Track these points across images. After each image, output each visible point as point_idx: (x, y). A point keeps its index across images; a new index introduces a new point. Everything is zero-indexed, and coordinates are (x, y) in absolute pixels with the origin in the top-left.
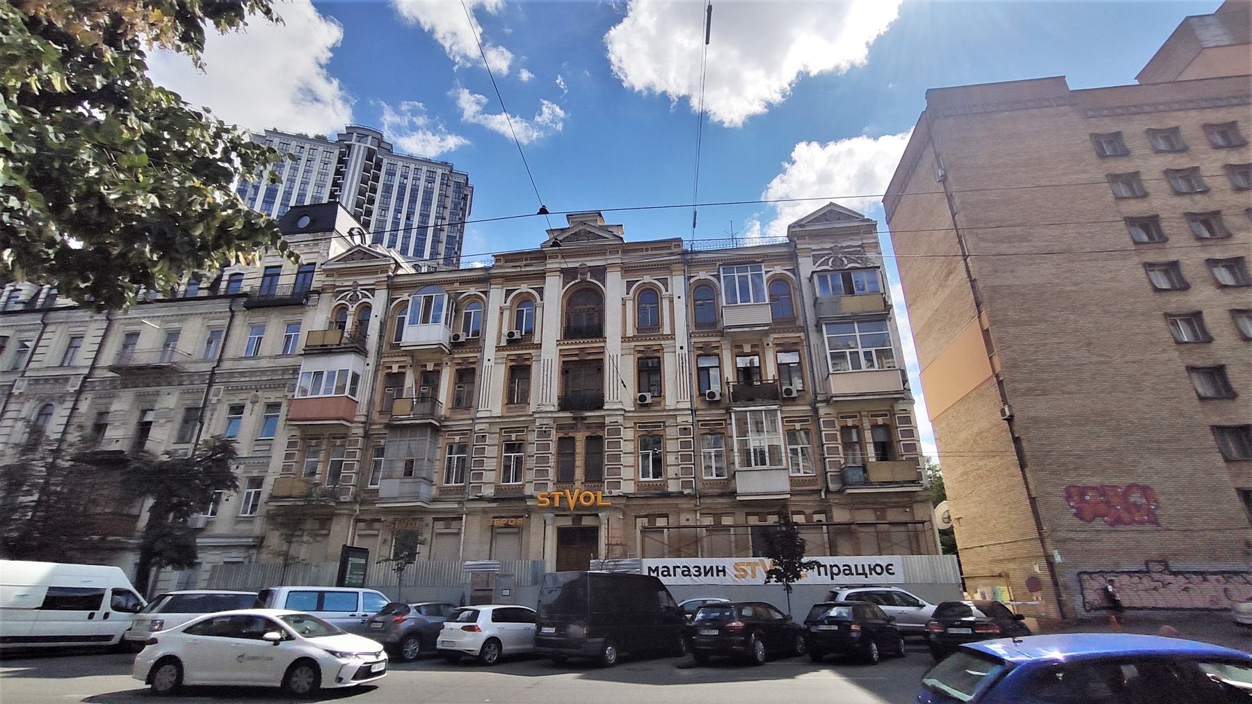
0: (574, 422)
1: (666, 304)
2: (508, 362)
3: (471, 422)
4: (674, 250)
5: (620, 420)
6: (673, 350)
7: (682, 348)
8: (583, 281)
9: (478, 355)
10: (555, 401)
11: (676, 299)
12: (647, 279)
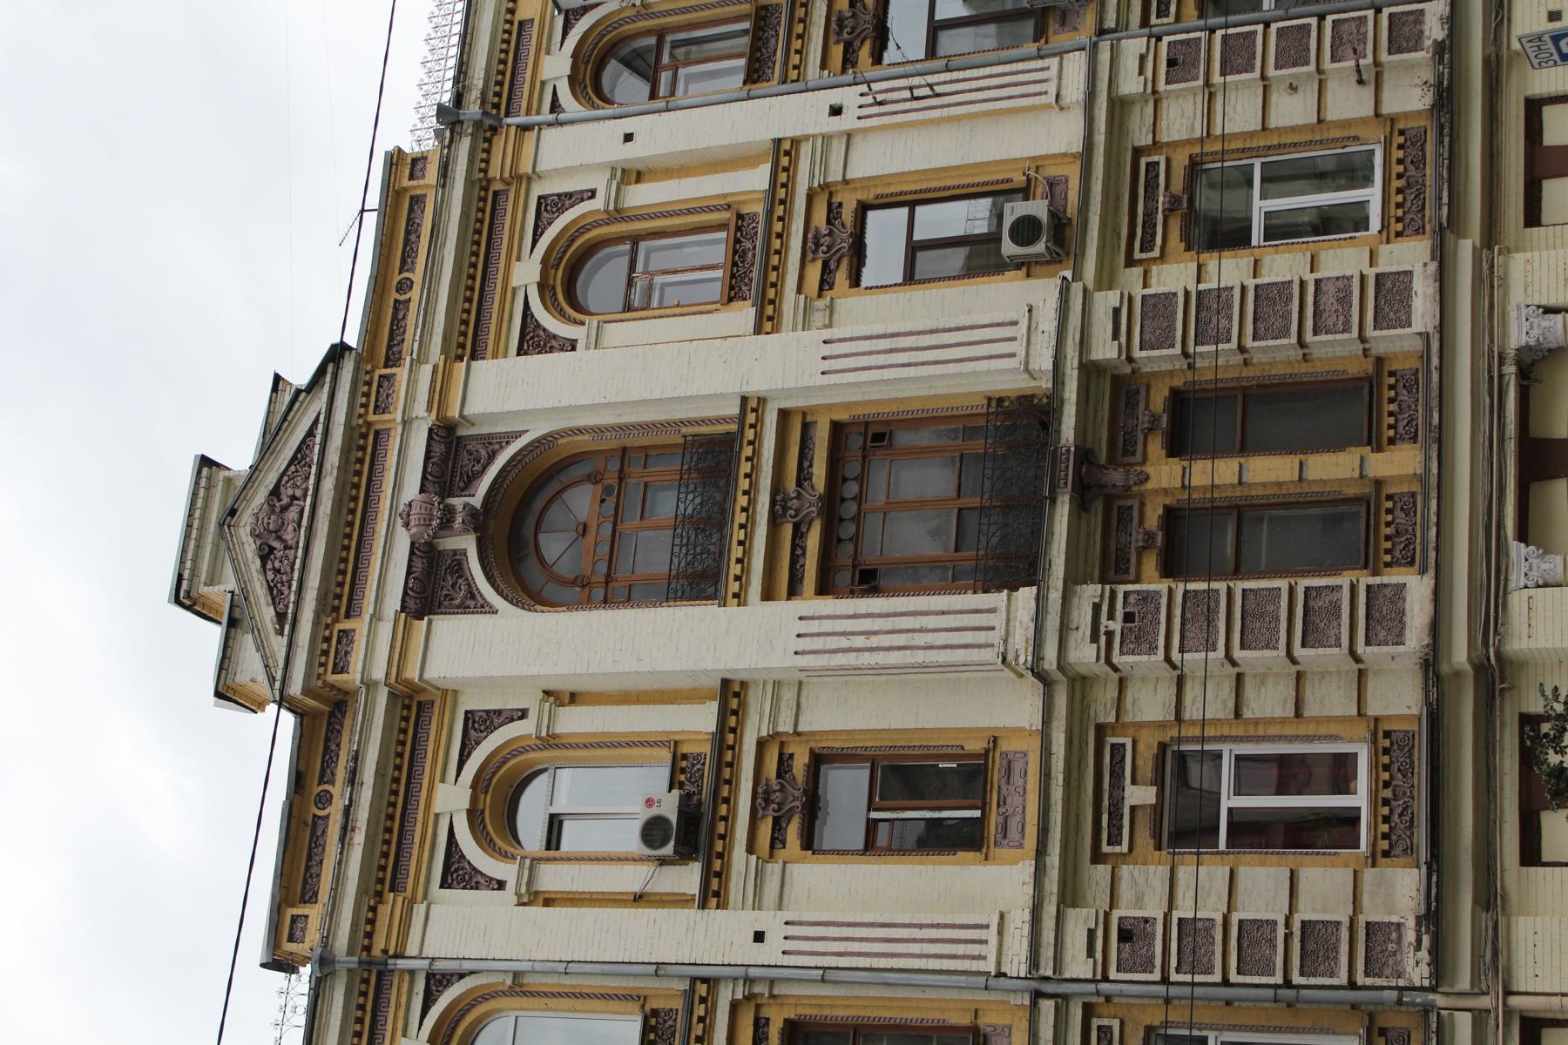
0: (1098, 506)
1: (641, 196)
2: (781, 854)
3: (1047, 1006)
4: (432, 174)
5: (1106, 301)
6: (838, 148)
7: (836, 111)
8: (478, 521)
9: (725, 997)
10: (998, 599)
11: (633, 152)
12: (526, 273)
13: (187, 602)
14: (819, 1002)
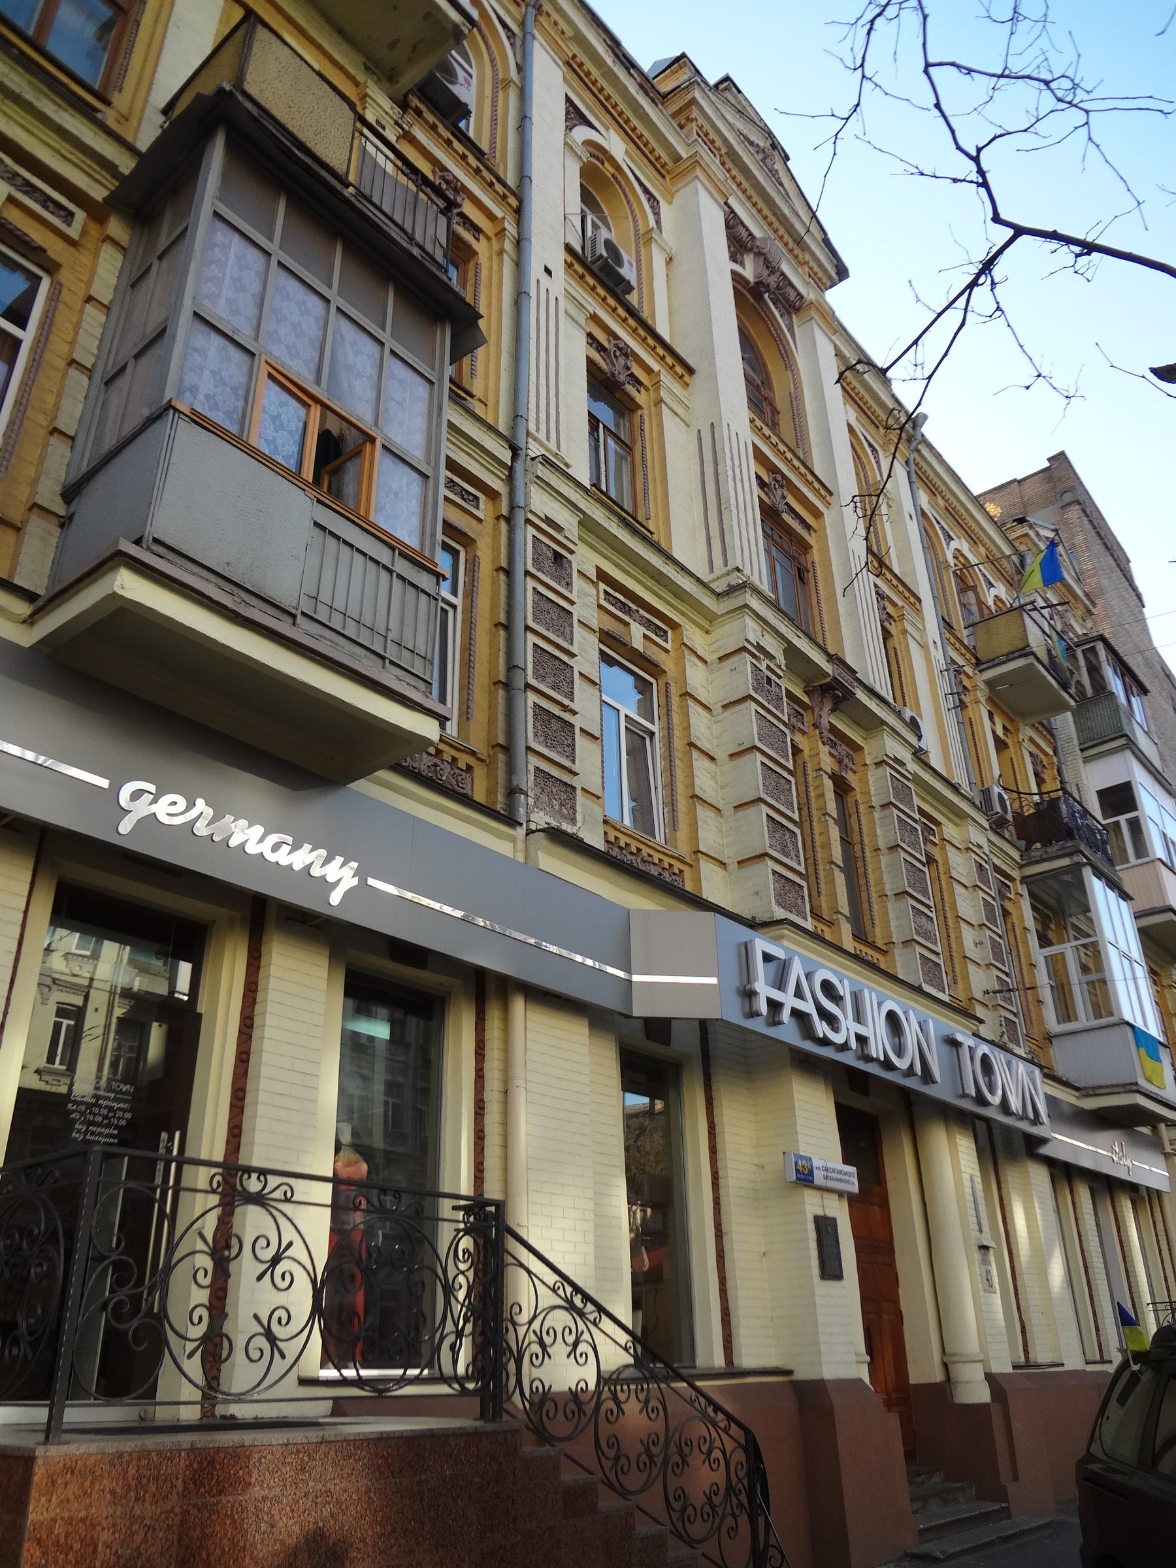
13: (721, 87)
14: (494, 286)
